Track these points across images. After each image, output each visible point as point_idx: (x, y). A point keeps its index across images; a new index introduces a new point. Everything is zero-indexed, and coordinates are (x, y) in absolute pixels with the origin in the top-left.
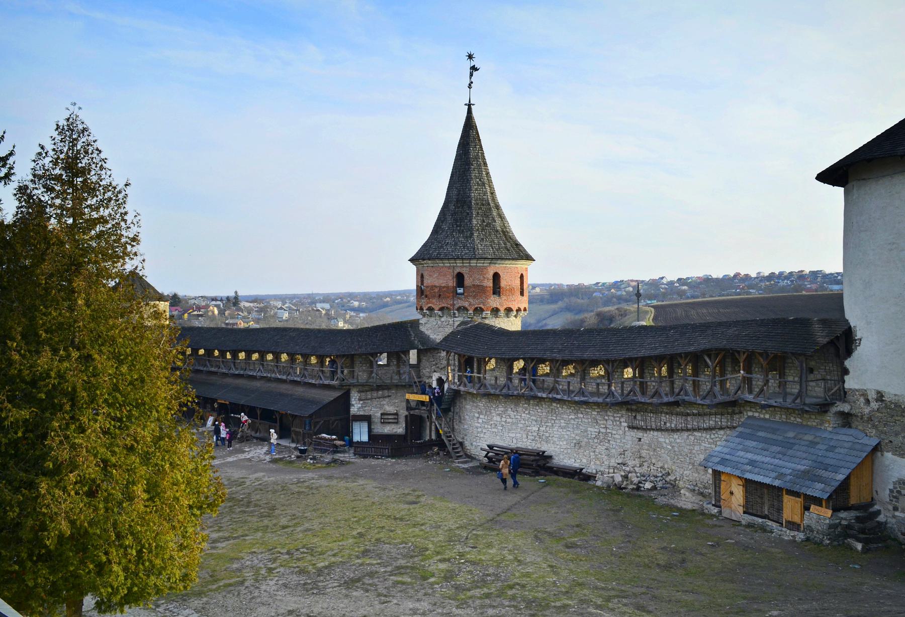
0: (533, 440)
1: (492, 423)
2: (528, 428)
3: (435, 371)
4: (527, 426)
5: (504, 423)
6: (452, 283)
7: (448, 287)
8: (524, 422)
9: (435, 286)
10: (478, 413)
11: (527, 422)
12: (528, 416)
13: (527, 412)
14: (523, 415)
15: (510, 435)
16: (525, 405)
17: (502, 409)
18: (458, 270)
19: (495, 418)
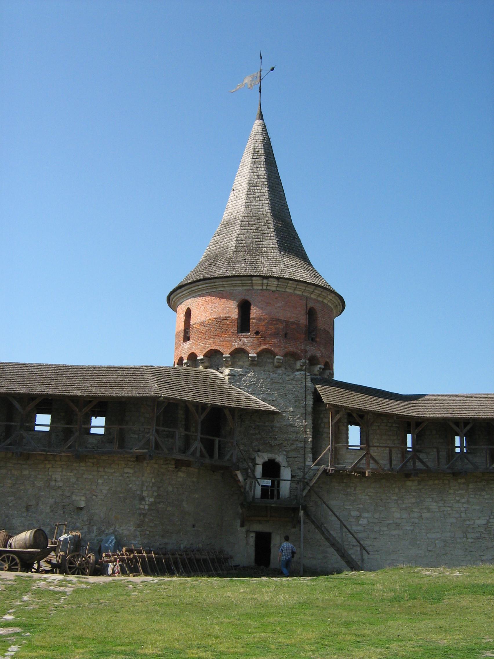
0: (477, 538)
1: (391, 522)
2: (468, 523)
3: (259, 451)
4: (464, 520)
5: (416, 521)
6: (303, 320)
7: (298, 325)
8: (457, 515)
9: (278, 320)
10: (358, 510)
11: (463, 515)
12: (465, 506)
13: (463, 500)
14: (456, 505)
15: (429, 536)
16: (460, 492)
17: (413, 500)
18: (310, 305)
19: (397, 515)
